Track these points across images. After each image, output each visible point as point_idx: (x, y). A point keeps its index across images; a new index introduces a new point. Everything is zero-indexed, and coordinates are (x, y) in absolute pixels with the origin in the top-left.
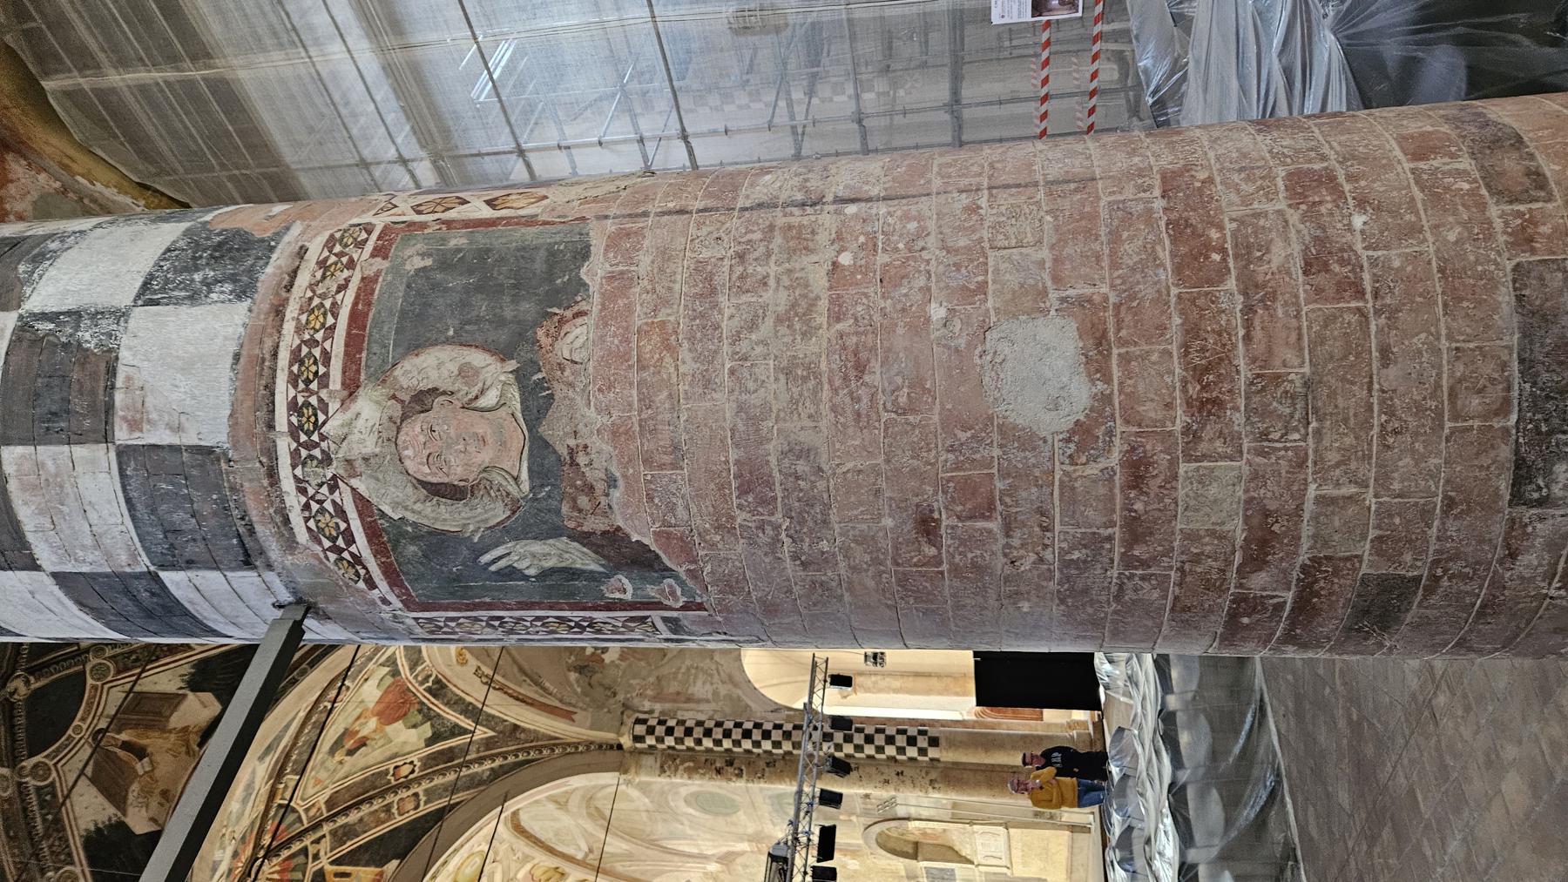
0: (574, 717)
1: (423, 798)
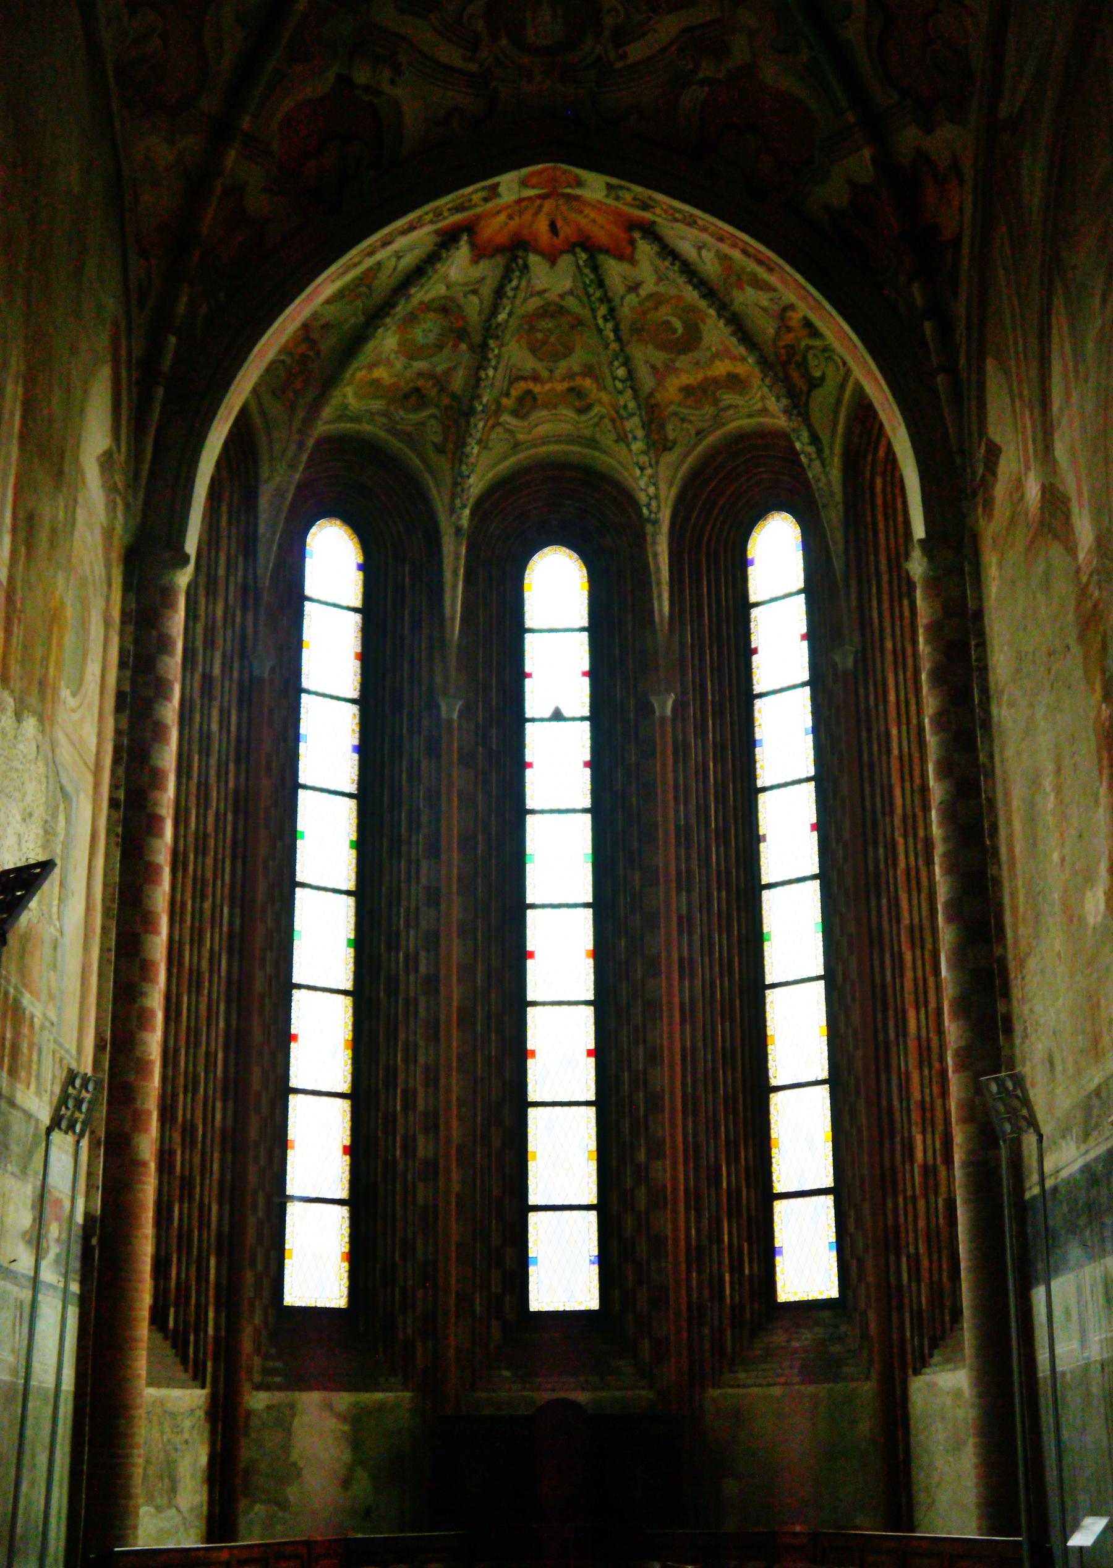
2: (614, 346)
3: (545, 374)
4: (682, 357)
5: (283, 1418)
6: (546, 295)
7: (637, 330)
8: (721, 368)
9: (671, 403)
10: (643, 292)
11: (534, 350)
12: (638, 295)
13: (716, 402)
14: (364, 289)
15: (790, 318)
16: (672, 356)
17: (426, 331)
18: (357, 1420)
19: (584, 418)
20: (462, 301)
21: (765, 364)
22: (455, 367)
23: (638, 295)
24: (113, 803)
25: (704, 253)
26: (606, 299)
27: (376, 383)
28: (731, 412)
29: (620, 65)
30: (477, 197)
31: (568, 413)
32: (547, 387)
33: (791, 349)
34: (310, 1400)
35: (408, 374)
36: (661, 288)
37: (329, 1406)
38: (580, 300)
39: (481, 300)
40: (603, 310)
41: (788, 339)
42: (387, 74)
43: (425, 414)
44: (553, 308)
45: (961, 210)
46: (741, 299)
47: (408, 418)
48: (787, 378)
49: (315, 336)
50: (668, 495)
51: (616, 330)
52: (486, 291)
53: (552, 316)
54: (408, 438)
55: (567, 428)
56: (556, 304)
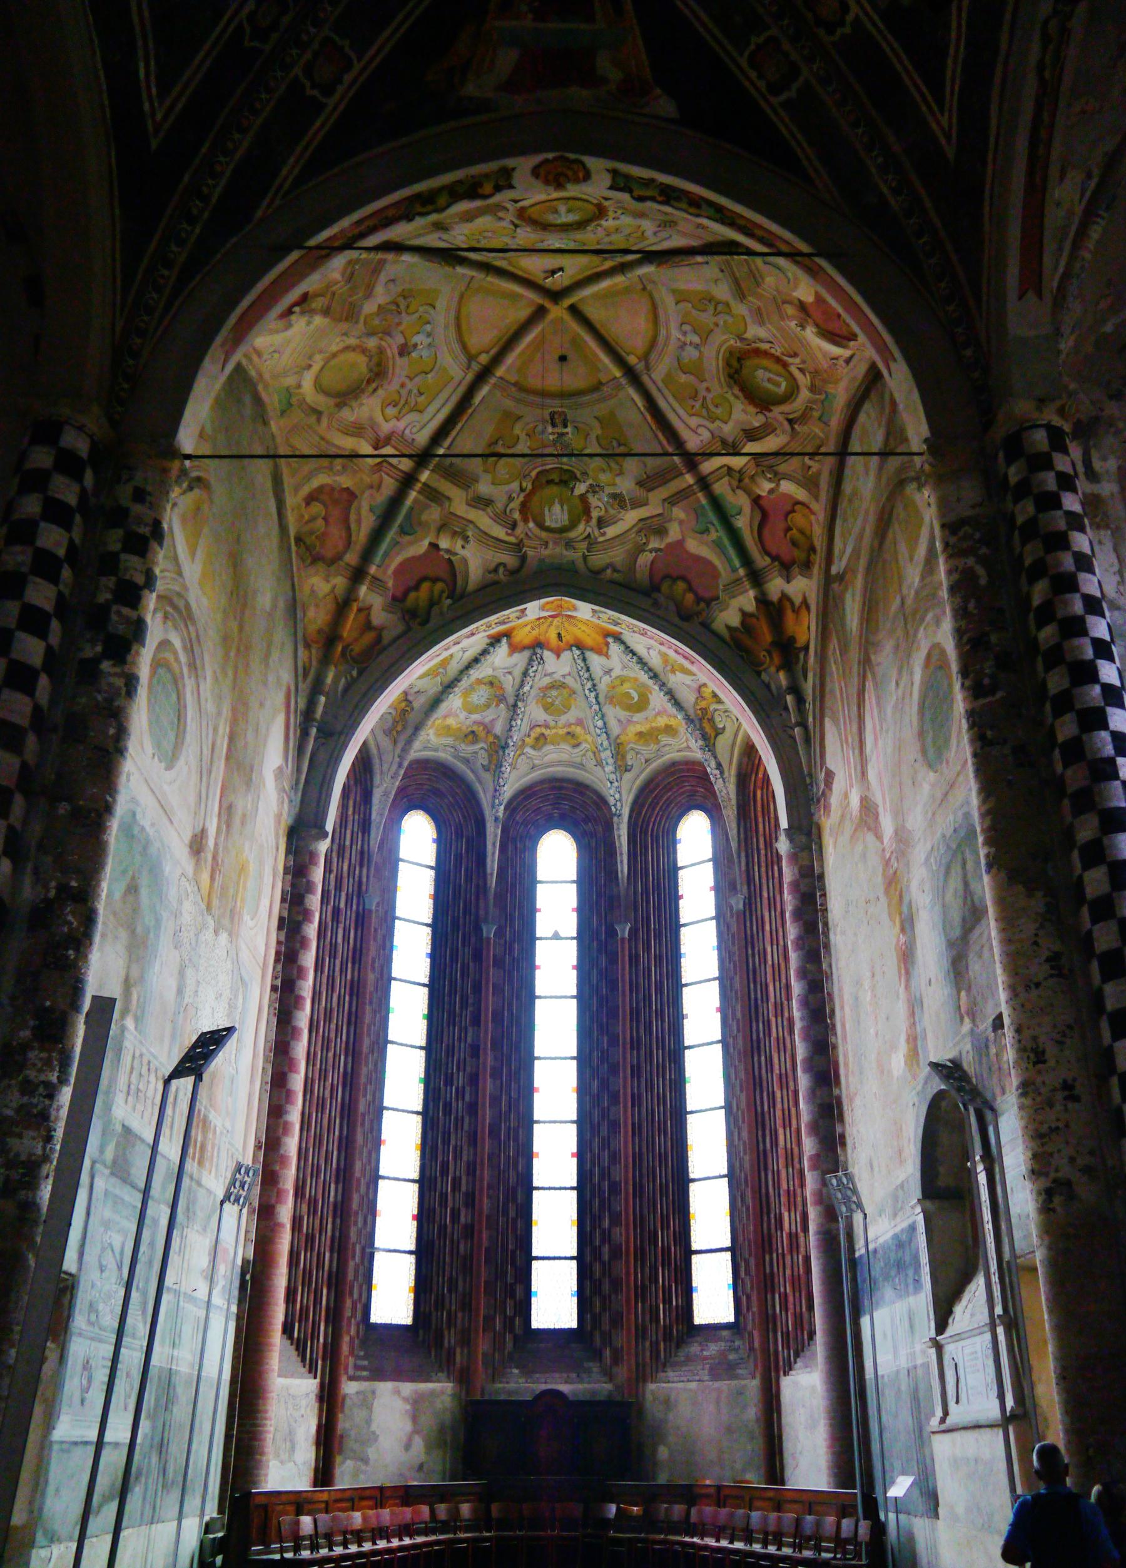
0: (1031, 296)
1: (792, 93)
2: (596, 707)
3: (552, 724)
5: (366, 1401)
7: (611, 699)
8: (661, 722)
10: (614, 674)
11: (546, 709)
13: (658, 742)
17: (481, 695)
18: (417, 1402)
19: (577, 750)
20: (502, 679)
21: (689, 720)
24: (274, 988)
26: (590, 678)
27: (448, 727)
28: (667, 748)
29: (601, 539)
30: (513, 616)
32: (554, 731)
33: (704, 710)
34: (385, 1388)
35: (468, 722)
36: (625, 673)
37: (397, 1392)
40: (589, 685)
41: (703, 704)
42: (460, 543)
45: (809, 628)
47: (467, 749)
48: (702, 729)
49: (410, 698)
50: (628, 799)
51: (596, 698)
52: (518, 672)
54: (467, 761)
55: (564, 757)
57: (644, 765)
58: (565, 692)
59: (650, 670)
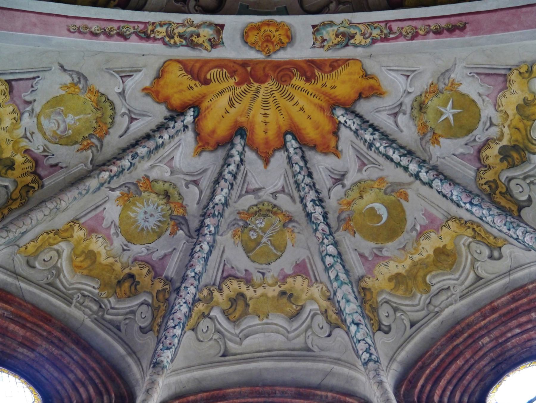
2: (322, 226)
3: (257, 278)
4: (390, 244)
6: (260, 194)
9: (382, 291)
10: (348, 182)
12: (344, 186)
14: (94, 141)
15: (487, 157)
16: (379, 245)
19: (295, 325)
22: (171, 253)
23: (344, 186)
25: (401, 118)
26: (313, 186)
27: (92, 256)
28: (443, 297)
31: (281, 321)
32: (260, 291)
33: (494, 185)
35: (126, 257)
36: (365, 175)
38: (292, 198)
39: (201, 192)
41: (489, 176)
43: (135, 302)
44: (266, 207)
46: (438, 154)
49: (42, 172)
51: (325, 216)
52: (206, 182)
53: (265, 216)
55: (278, 340)
56: (269, 203)
57: (409, 331)
58: (277, 220)
59: (401, 147)
